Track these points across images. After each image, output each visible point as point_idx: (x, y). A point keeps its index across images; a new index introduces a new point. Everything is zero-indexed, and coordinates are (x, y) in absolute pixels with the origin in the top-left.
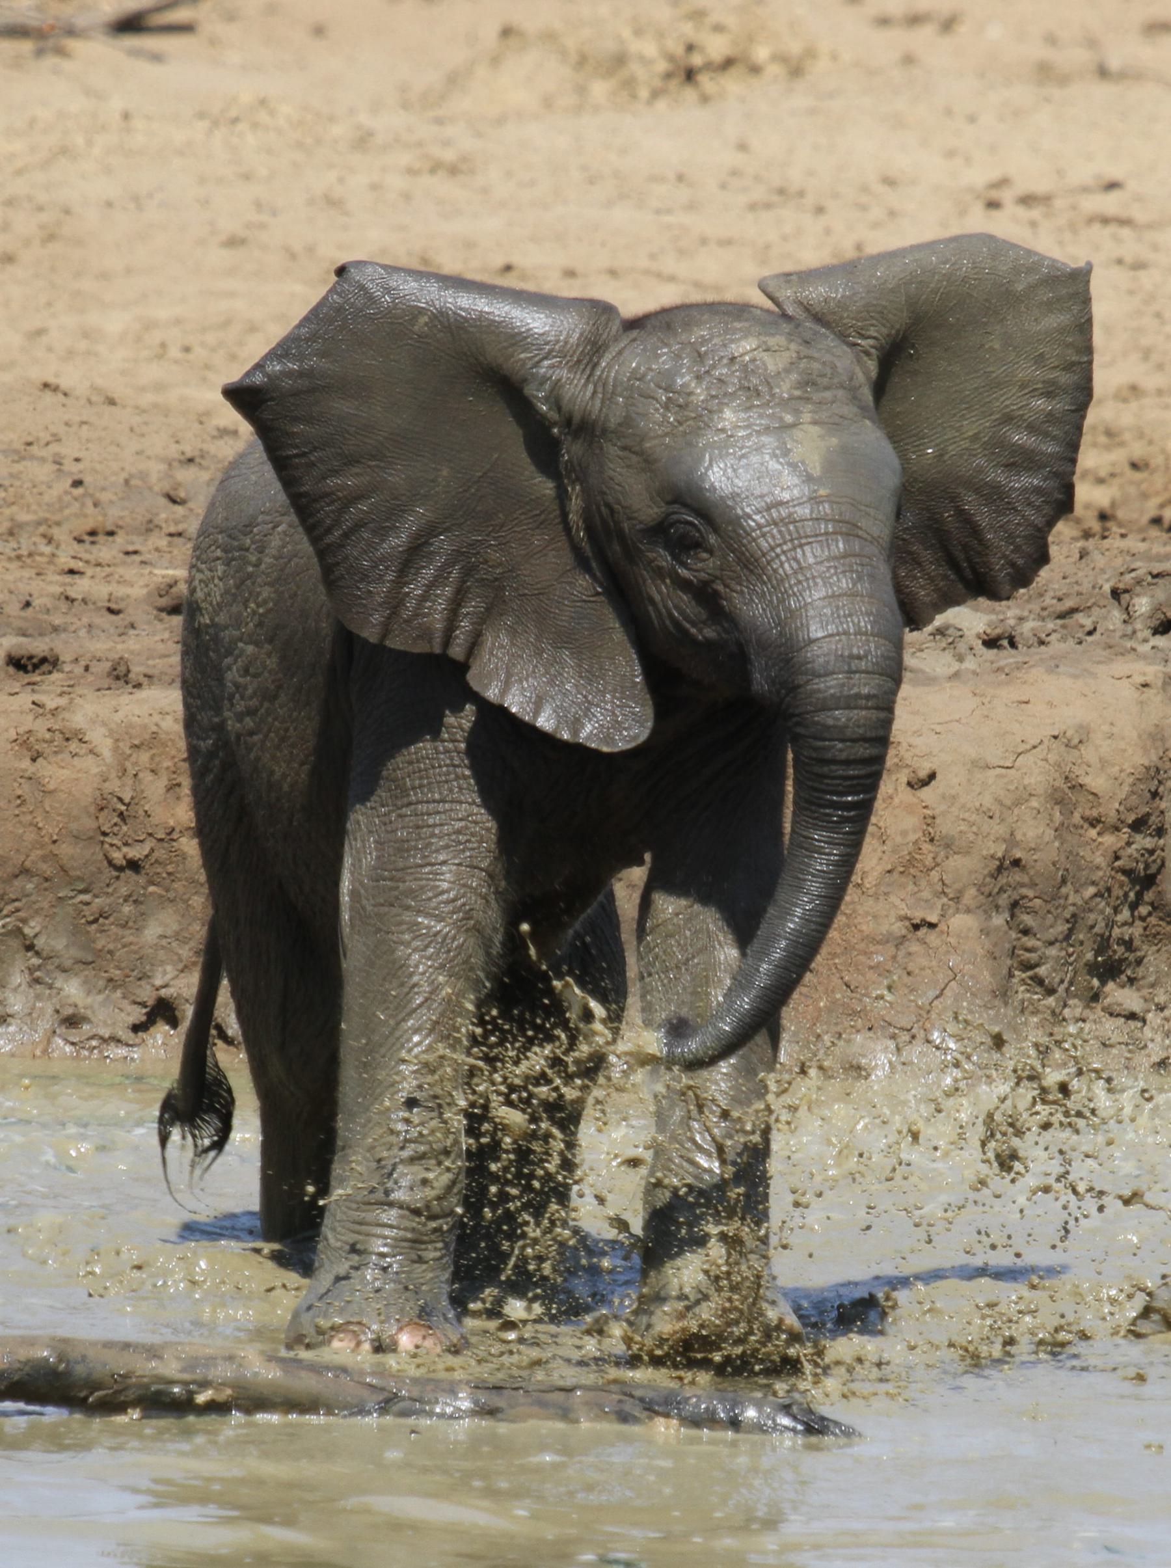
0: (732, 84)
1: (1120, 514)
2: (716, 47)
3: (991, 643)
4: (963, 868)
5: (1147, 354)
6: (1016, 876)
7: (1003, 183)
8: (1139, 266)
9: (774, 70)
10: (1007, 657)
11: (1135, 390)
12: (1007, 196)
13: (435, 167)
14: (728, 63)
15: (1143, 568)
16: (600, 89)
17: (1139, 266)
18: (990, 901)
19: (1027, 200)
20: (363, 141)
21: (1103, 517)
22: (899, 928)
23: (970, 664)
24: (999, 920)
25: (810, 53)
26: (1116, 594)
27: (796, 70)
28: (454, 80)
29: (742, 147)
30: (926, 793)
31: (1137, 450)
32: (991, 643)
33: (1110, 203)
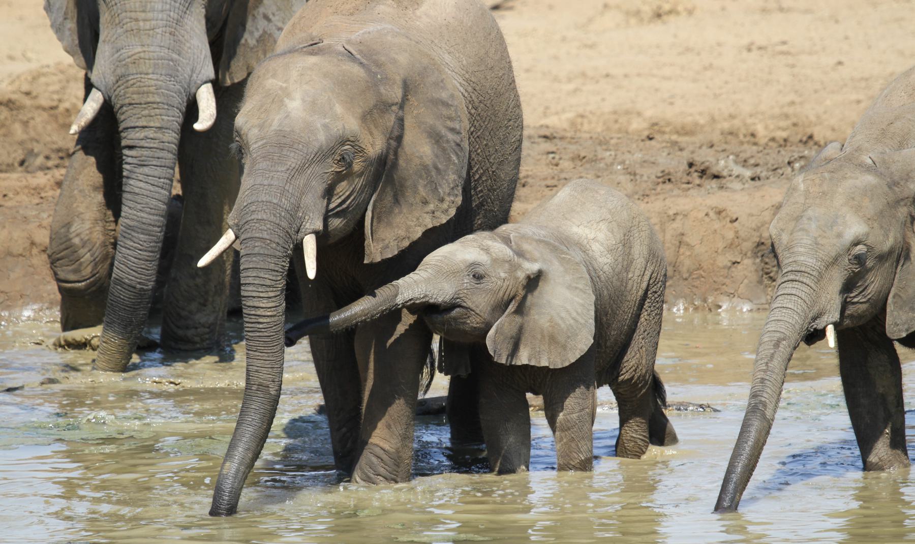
0: (672, 18)
1: (791, 139)
2: (667, 7)
3: (753, 179)
4: (748, 245)
5: (796, 92)
6: (763, 247)
7: (752, 44)
8: (793, 66)
9: (684, 14)
10: (757, 183)
11: (793, 103)
12: (754, 47)
13: (586, 46)
14: (670, 12)
15: (796, 155)
16: (633, 21)
17: (793, 66)
18: (755, 255)
19: (760, 48)
20: (564, 39)
21: (785, 140)
22: (729, 264)
23: (747, 186)
24: (758, 260)
25: (694, 8)
26: (789, 163)
27: (690, 12)
28: (590, 20)
29: (675, 36)
30: (736, 224)
31: (795, 120)
32: (753, 179)
33: (784, 48)
